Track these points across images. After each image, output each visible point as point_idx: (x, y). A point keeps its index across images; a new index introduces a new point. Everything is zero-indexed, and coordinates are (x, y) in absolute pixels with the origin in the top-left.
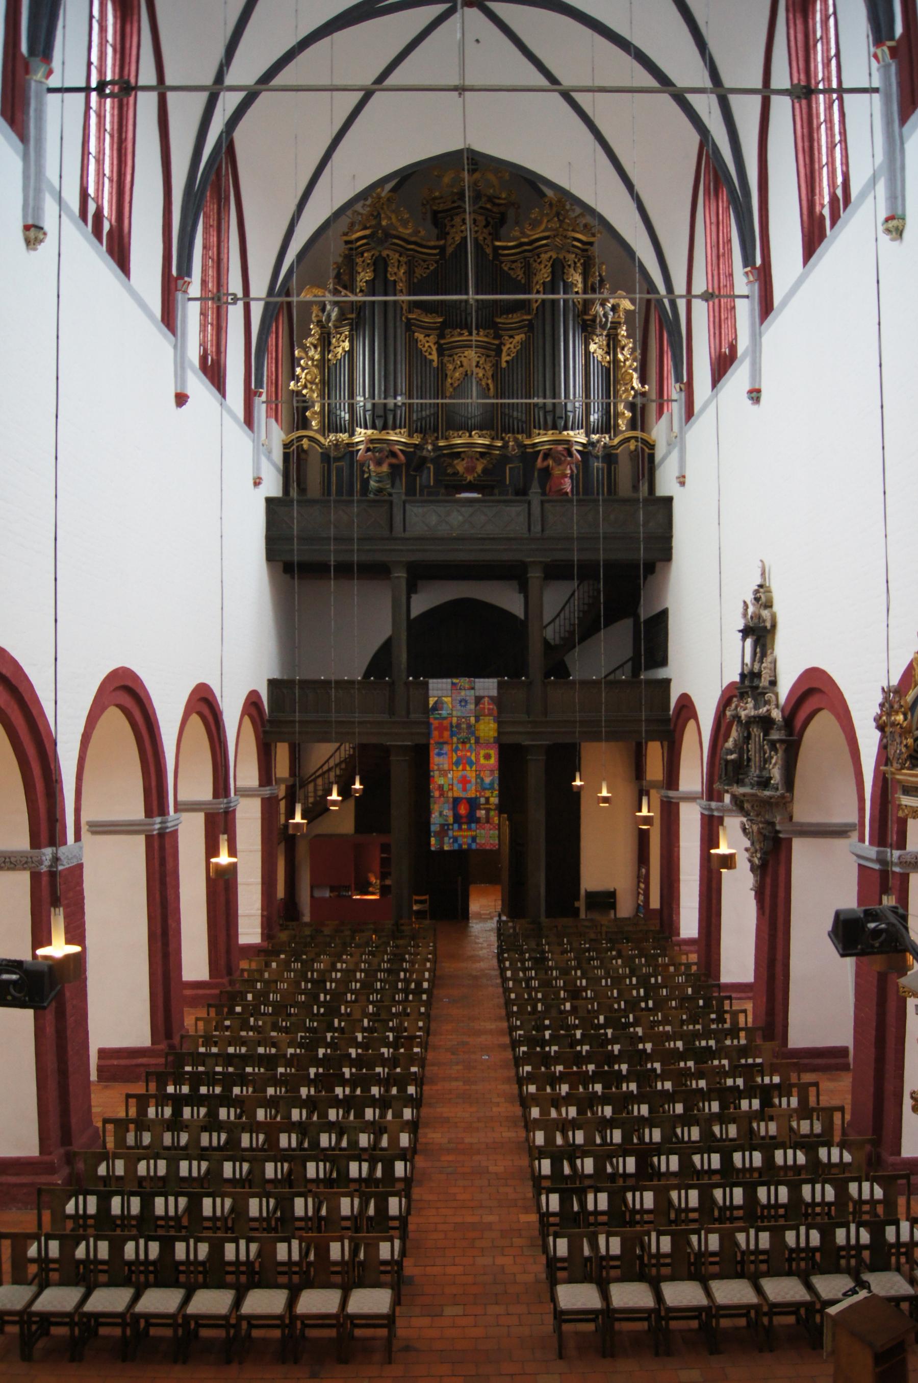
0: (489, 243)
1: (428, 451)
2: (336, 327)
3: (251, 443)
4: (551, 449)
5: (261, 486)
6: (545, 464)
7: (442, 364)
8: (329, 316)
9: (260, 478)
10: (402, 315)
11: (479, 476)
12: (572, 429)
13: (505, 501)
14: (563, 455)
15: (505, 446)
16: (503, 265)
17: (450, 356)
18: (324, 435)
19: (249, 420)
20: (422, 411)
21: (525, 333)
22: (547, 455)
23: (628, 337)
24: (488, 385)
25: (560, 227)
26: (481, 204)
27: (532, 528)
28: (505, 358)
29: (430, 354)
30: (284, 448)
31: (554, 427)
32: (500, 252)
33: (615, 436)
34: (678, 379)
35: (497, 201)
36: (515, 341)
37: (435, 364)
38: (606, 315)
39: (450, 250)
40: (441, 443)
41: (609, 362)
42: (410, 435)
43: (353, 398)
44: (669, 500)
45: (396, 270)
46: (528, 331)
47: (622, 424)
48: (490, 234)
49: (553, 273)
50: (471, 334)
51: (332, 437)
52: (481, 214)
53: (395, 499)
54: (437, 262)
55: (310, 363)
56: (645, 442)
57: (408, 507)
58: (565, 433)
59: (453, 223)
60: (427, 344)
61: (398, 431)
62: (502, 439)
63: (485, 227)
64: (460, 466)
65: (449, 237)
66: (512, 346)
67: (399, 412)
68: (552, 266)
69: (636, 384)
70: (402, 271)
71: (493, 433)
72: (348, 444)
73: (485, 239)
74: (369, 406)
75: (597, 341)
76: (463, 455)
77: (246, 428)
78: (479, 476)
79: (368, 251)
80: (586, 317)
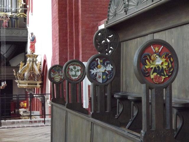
12: (8, 12)
47: (19, 11)
58: (6, 13)
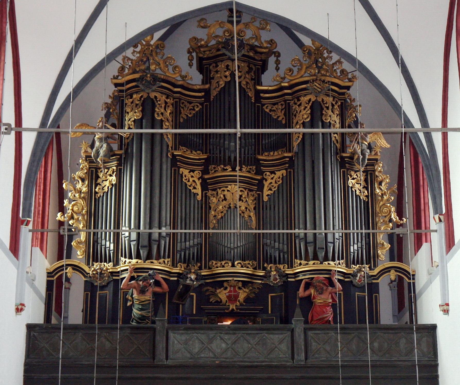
0: (252, 88)
1: (191, 280)
2: (105, 162)
3: (16, 271)
4: (313, 278)
5: (23, 313)
6: (307, 293)
7: (206, 198)
8: (98, 153)
9: (23, 305)
10: (168, 151)
11: (241, 305)
12: (333, 260)
13: (268, 329)
14: (324, 284)
15: (267, 276)
16: (264, 107)
17: (214, 190)
18: (88, 264)
19: (14, 248)
20: (185, 241)
21: (286, 169)
22: (308, 285)
23: (385, 173)
24: (250, 216)
25: (318, 73)
26: (243, 52)
27: (296, 356)
28: (266, 192)
29: (194, 188)
30: (48, 277)
31: (315, 258)
32: (262, 95)
33: (375, 266)
34: (437, 210)
35: (259, 50)
36: (276, 177)
37: (199, 197)
38: (363, 154)
39: (214, 93)
40: (204, 273)
41: (367, 196)
42: (174, 265)
43: (118, 228)
44: (433, 328)
45: (162, 110)
46: (289, 167)
48: (252, 79)
49: (312, 114)
50: (234, 170)
51: (96, 266)
52: (244, 61)
53: (158, 326)
54: (202, 104)
55: (77, 195)
56: (406, 273)
57: (171, 335)
58: (326, 263)
59: (218, 68)
60: (192, 178)
61: (161, 260)
62: (264, 269)
63: (248, 72)
64: (223, 295)
65: (214, 82)
66: (273, 181)
67: (163, 242)
68: (311, 108)
69: (394, 216)
70: (169, 111)
71: (255, 263)
72: (111, 273)
73: (247, 83)
74: (134, 236)
75: (355, 176)
76: (225, 284)
77: (11, 255)
78: (241, 305)
79: (136, 93)
80: (344, 155)
